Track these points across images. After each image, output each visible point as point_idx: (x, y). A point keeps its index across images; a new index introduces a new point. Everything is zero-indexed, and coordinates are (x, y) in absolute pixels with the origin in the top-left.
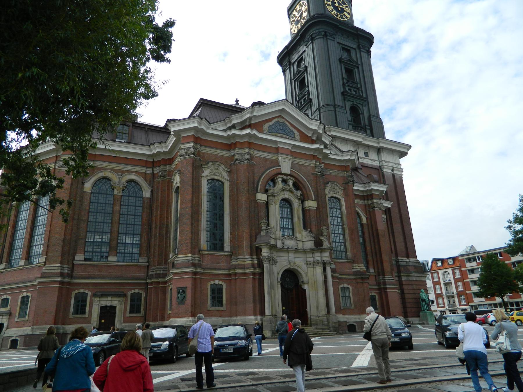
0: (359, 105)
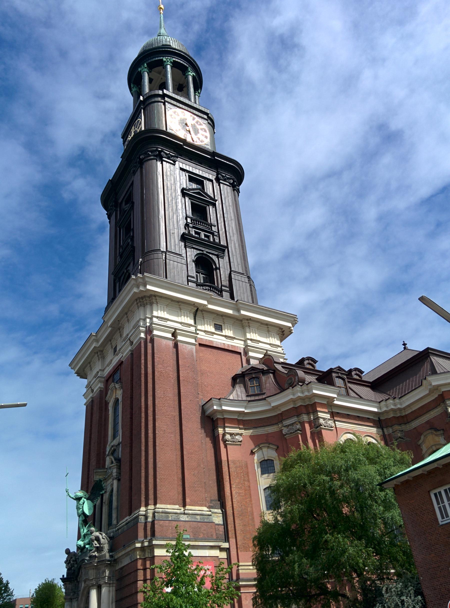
0: (211, 255)
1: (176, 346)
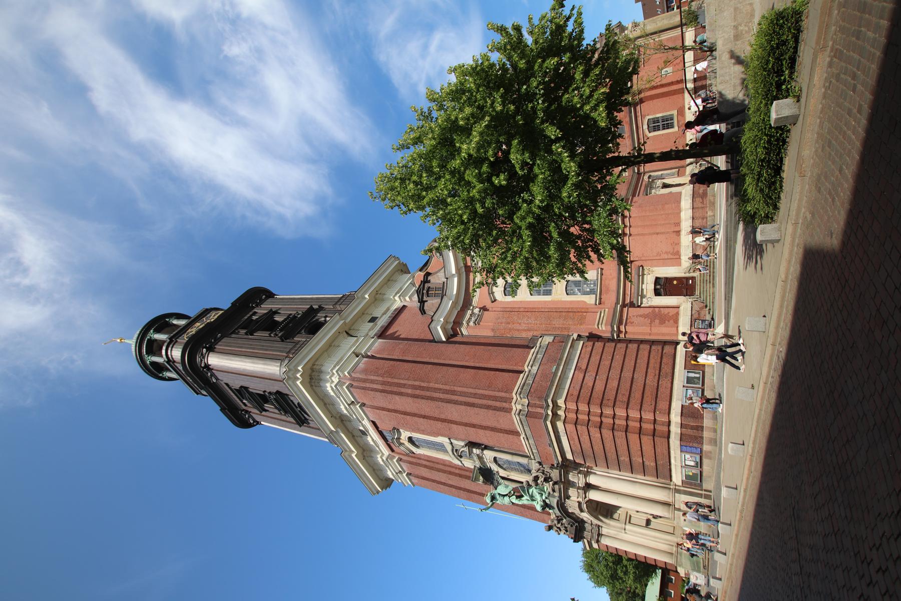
1: (368, 357)
